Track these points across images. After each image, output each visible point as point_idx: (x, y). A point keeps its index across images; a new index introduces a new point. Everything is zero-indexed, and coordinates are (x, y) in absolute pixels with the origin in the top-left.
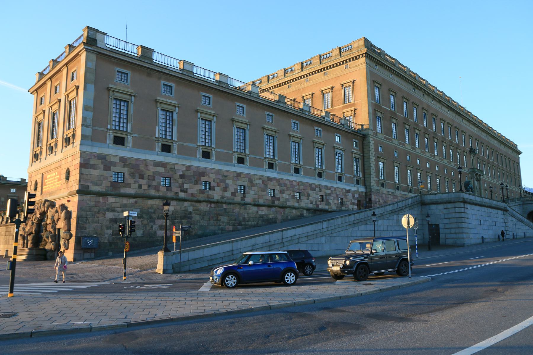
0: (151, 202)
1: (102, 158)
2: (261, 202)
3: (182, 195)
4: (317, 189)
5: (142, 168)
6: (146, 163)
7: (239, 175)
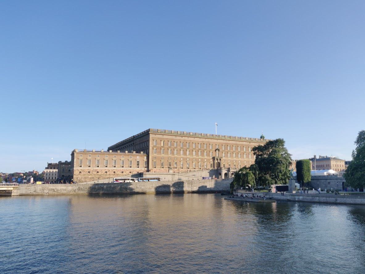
0: (86, 176)
1: (77, 170)
2: (111, 174)
3: (92, 174)
4: (129, 170)
5: (84, 170)
6: (85, 169)
7: (105, 169)
